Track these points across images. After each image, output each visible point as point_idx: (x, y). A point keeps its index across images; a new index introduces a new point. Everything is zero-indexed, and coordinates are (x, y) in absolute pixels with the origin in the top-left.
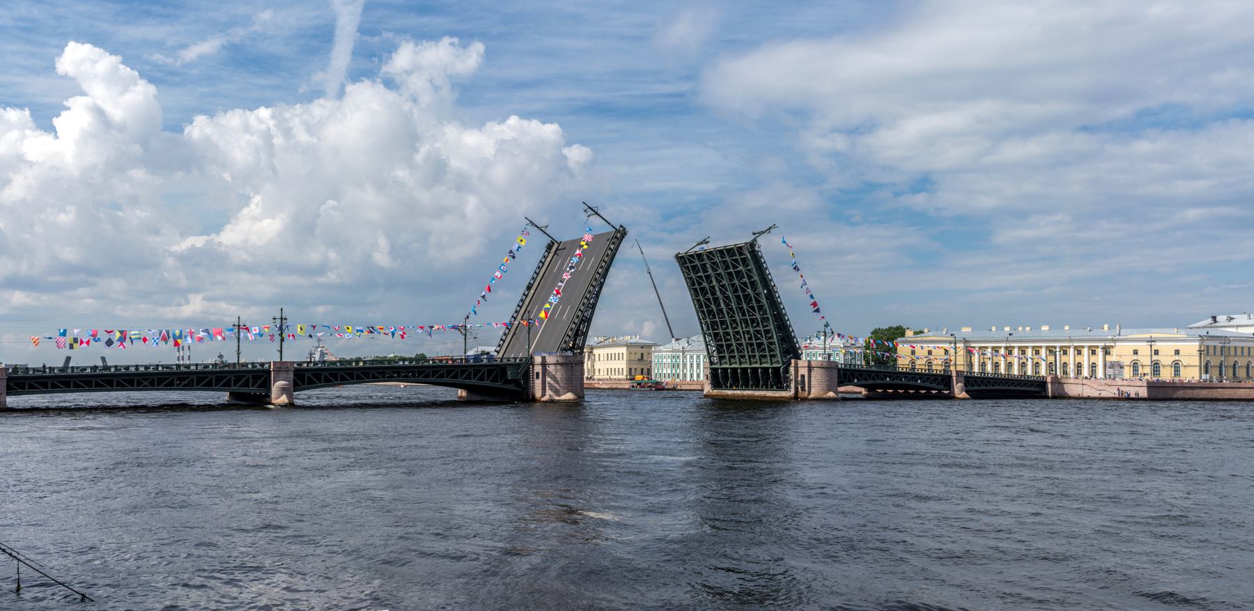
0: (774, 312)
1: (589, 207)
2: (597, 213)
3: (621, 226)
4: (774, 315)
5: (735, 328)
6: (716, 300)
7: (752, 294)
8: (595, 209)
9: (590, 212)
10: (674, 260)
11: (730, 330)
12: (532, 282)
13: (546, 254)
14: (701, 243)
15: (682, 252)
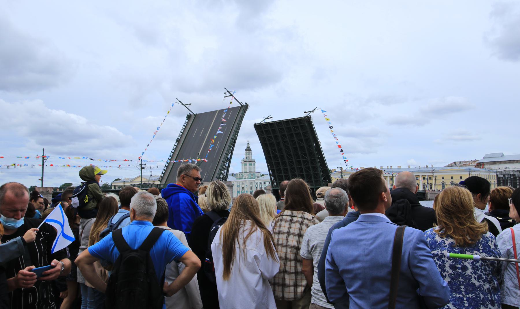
0: (318, 156)
1: (228, 91)
2: (232, 95)
3: (246, 103)
4: (319, 158)
5: (292, 166)
6: (280, 150)
7: (305, 146)
8: (232, 93)
9: (228, 94)
10: (253, 127)
11: (288, 167)
12: (179, 138)
13: (187, 121)
14: (266, 118)
15: (258, 121)
